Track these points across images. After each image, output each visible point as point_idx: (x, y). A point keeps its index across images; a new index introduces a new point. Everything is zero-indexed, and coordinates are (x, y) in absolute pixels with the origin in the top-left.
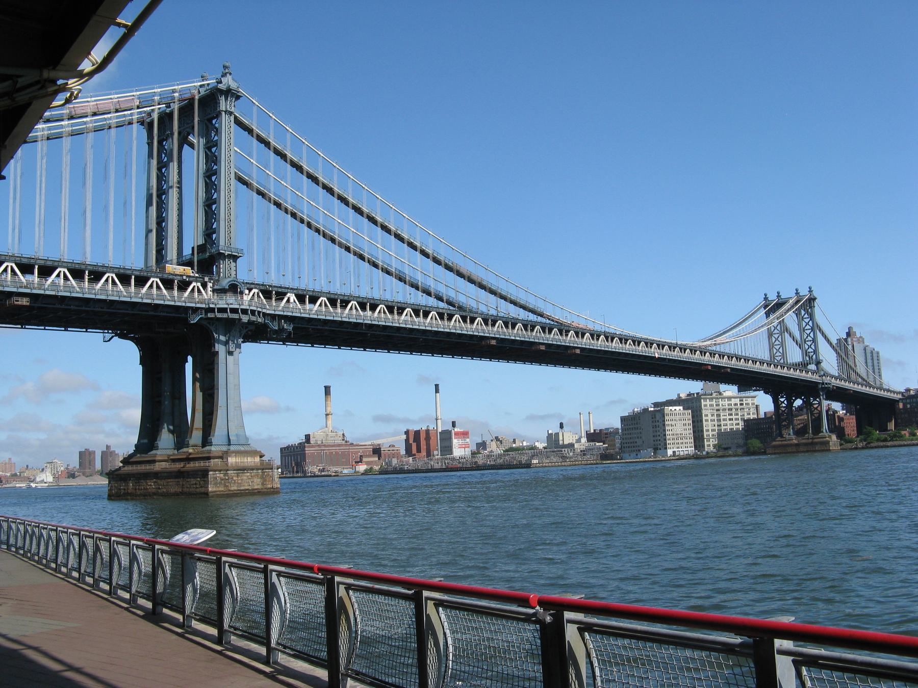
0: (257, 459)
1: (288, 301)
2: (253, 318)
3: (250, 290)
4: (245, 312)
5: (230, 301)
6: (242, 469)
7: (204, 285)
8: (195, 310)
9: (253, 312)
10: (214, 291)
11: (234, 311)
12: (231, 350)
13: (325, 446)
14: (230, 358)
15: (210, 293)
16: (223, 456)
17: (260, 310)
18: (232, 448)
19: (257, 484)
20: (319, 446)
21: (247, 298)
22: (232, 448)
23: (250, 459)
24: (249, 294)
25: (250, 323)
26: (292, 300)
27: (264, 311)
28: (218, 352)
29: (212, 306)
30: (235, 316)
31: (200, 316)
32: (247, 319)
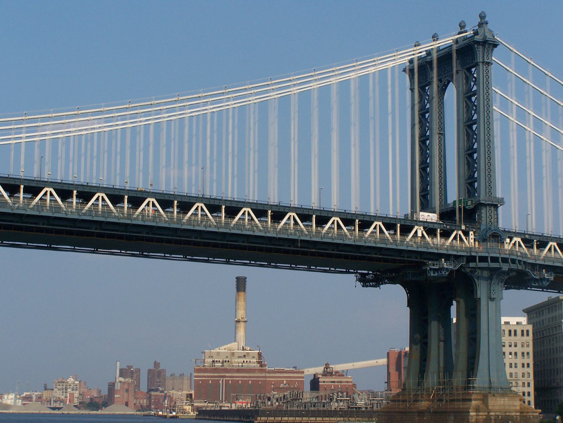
2: (513, 266)
3: (511, 239)
4: (505, 260)
9: (513, 261)
11: (495, 260)
12: (492, 296)
14: (492, 304)
17: (520, 259)
21: (508, 246)
24: (510, 243)
25: (511, 270)
27: (525, 260)
28: (480, 299)
29: (473, 254)
31: (462, 263)
32: (508, 267)
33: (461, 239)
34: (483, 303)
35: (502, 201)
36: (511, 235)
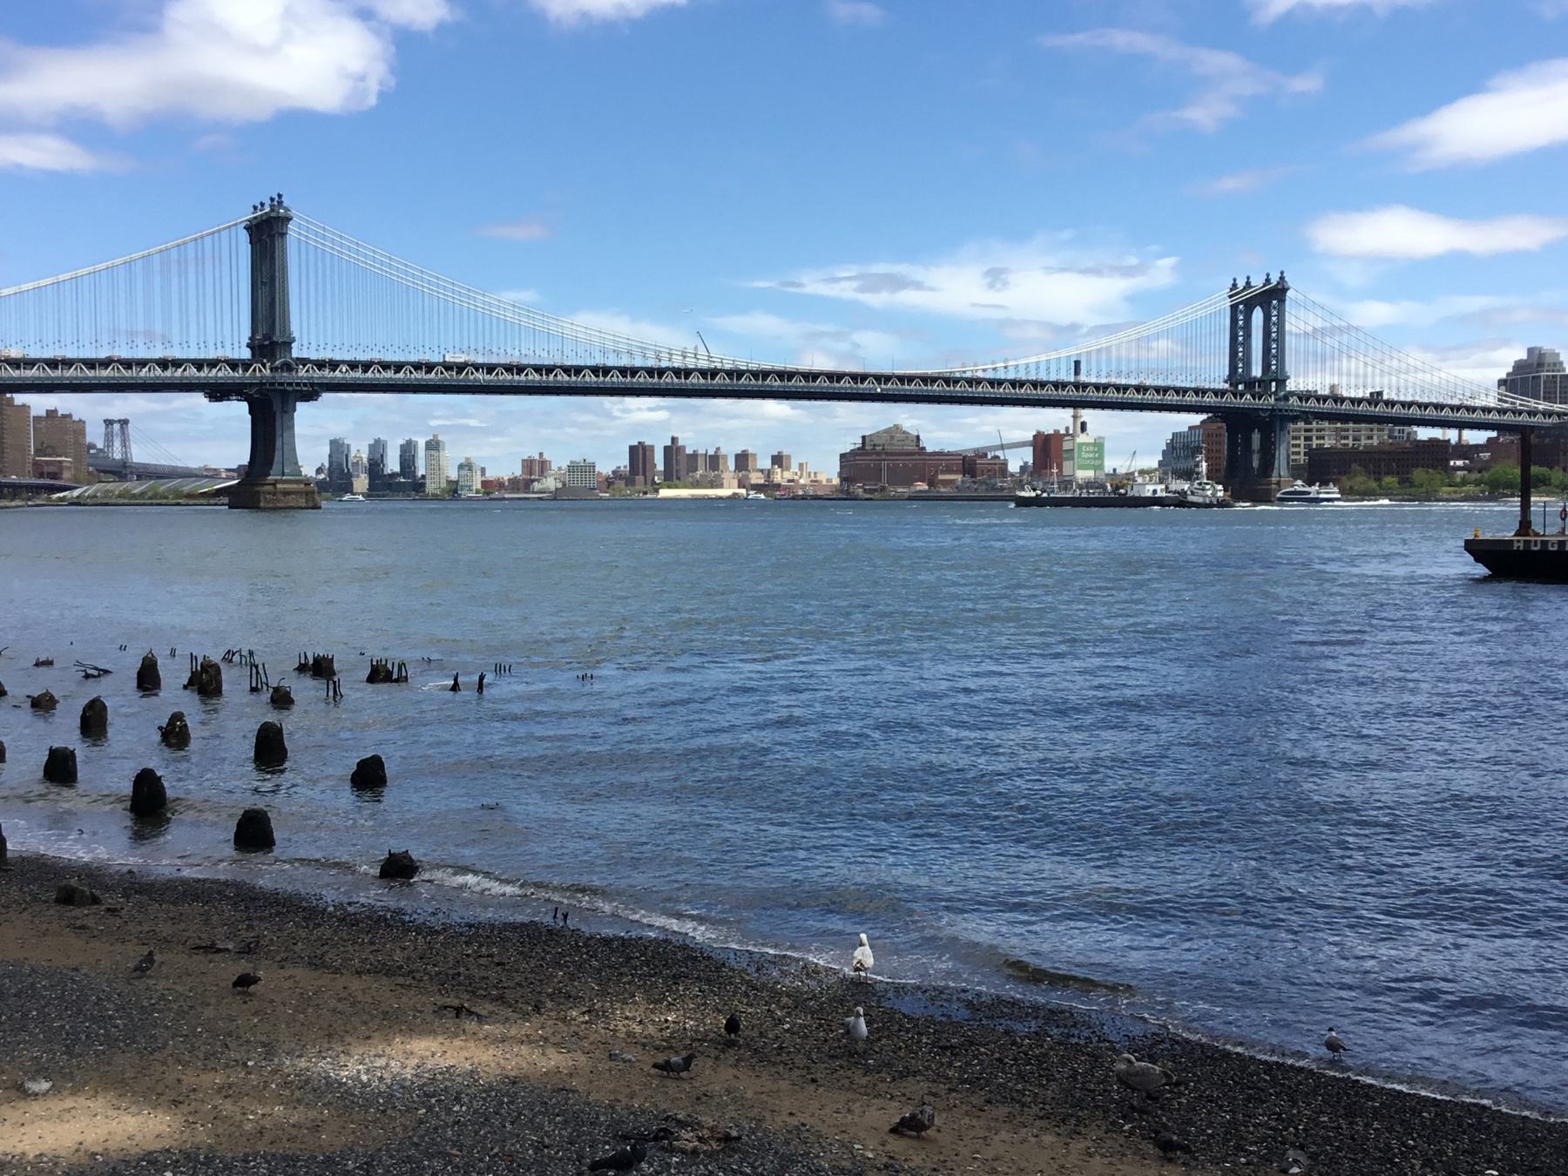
0: (302, 486)
1: (340, 371)
3: (304, 366)
5: (285, 376)
6: (286, 493)
7: (265, 367)
8: (251, 385)
10: (271, 370)
13: (887, 454)
15: (269, 371)
16: (274, 485)
18: (284, 478)
19: (302, 502)
20: (878, 454)
22: (284, 478)
23: (295, 486)
26: (344, 370)
30: (282, 388)
33: (260, 371)
34: (278, 415)
35: (294, 340)
36: (304, 362)
